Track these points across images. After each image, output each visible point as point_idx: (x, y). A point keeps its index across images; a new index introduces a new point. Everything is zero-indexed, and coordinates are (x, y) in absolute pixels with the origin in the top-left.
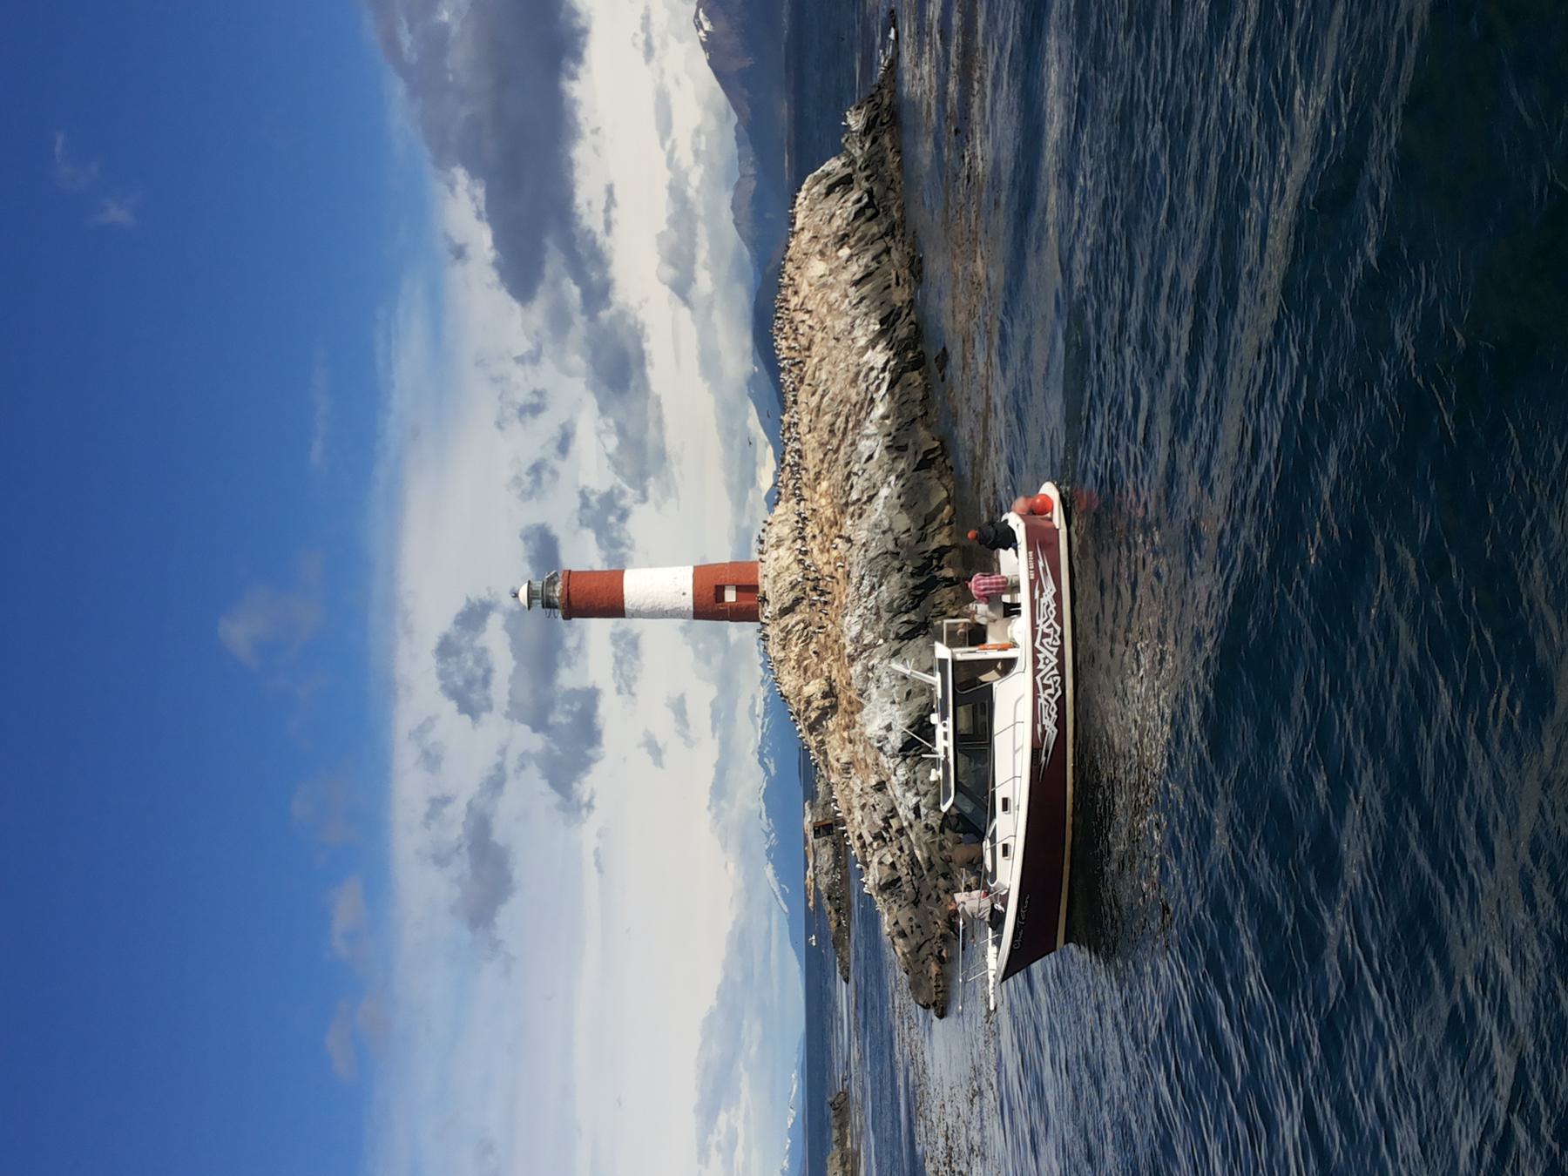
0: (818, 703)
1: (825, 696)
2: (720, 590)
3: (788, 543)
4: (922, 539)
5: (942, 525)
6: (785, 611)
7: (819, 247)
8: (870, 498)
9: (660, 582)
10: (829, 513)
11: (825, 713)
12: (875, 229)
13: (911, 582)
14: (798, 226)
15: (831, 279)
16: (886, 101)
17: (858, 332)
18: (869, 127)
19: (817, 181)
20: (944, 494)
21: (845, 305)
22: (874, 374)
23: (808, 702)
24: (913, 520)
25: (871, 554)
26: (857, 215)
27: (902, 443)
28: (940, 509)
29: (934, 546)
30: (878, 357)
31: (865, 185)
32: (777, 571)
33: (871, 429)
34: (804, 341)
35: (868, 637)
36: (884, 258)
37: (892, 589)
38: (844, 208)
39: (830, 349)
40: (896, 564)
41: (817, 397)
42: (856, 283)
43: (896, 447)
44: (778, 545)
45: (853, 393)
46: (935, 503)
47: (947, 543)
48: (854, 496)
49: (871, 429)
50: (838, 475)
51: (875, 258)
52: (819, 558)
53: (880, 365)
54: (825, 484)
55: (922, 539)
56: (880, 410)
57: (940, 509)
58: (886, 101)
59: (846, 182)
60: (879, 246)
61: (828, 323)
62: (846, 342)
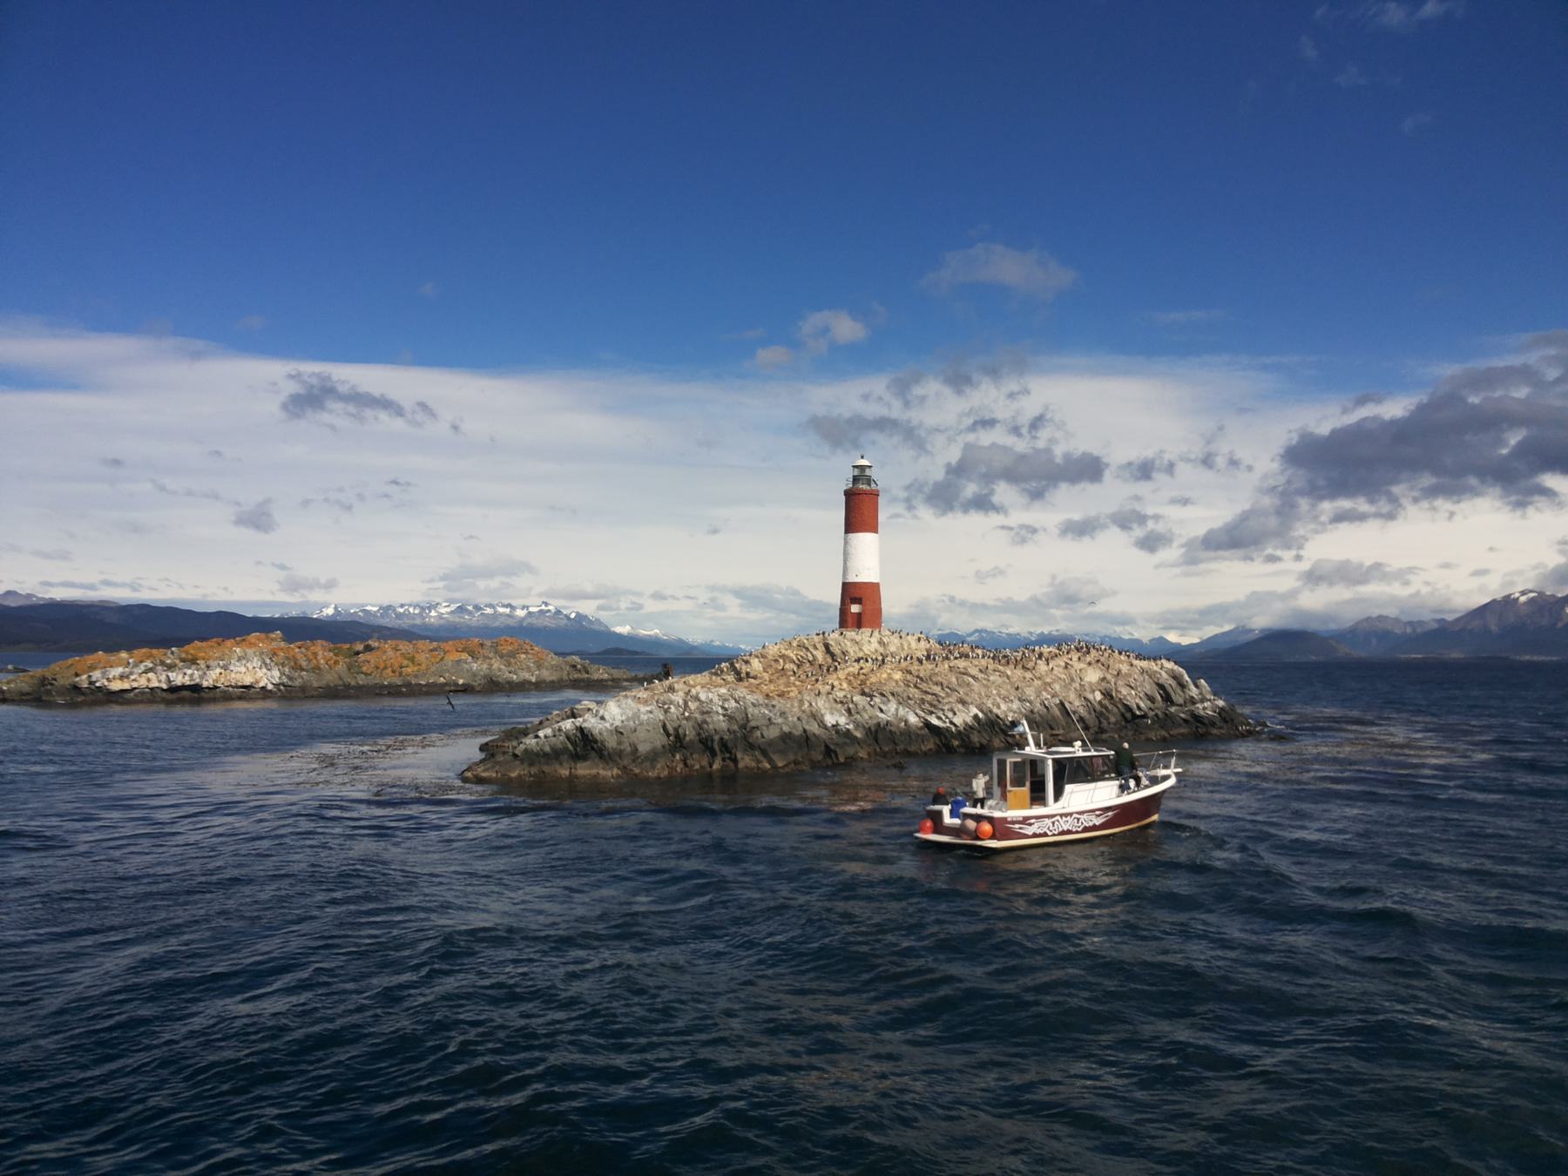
0: (745, 668)
1: (748, 674)
5: (759, 761)
7: (1109, 677)
8: (849, 711)
10: (873, 679)
11: (738, 673)
12: (1113, 719)
13: (716, 738)
16: (1215, 731)
17: (1016, 705)
18: (1197, 718)
19: (1175, 677)
20: (780, 764)
22: (950, 715)
23: (747, 662)
24: (771, 743)
25: (750, 710)
26: (1126, 706)
27: (880, 736)
28: (770, 761)
29: (739, 756)
30: (963, 718)
31: (1151, 714)
32: (867, 642)
33: (902, 712)
34: (1030, 665)
35: (693, 705)
37: (719, 722)
39: (1012, 684)
40: (735, 727)
41: (974, 671)
42: (1062, 704)
43: (878, 734)
44: (881, 642)
45: (953, 699)
46: (775, 757)
47: (741, 765)
48: (857, 698)
49: (902, 712)
50: (886, 689)
51: (1081, 719)
52: (841, 674)
53: (955, 720)
54: (898, 676)
56: (913, 719)
58: (1215, 731)
59: (1167, 698)
60: (1091, 720)
61: (1037, 682)
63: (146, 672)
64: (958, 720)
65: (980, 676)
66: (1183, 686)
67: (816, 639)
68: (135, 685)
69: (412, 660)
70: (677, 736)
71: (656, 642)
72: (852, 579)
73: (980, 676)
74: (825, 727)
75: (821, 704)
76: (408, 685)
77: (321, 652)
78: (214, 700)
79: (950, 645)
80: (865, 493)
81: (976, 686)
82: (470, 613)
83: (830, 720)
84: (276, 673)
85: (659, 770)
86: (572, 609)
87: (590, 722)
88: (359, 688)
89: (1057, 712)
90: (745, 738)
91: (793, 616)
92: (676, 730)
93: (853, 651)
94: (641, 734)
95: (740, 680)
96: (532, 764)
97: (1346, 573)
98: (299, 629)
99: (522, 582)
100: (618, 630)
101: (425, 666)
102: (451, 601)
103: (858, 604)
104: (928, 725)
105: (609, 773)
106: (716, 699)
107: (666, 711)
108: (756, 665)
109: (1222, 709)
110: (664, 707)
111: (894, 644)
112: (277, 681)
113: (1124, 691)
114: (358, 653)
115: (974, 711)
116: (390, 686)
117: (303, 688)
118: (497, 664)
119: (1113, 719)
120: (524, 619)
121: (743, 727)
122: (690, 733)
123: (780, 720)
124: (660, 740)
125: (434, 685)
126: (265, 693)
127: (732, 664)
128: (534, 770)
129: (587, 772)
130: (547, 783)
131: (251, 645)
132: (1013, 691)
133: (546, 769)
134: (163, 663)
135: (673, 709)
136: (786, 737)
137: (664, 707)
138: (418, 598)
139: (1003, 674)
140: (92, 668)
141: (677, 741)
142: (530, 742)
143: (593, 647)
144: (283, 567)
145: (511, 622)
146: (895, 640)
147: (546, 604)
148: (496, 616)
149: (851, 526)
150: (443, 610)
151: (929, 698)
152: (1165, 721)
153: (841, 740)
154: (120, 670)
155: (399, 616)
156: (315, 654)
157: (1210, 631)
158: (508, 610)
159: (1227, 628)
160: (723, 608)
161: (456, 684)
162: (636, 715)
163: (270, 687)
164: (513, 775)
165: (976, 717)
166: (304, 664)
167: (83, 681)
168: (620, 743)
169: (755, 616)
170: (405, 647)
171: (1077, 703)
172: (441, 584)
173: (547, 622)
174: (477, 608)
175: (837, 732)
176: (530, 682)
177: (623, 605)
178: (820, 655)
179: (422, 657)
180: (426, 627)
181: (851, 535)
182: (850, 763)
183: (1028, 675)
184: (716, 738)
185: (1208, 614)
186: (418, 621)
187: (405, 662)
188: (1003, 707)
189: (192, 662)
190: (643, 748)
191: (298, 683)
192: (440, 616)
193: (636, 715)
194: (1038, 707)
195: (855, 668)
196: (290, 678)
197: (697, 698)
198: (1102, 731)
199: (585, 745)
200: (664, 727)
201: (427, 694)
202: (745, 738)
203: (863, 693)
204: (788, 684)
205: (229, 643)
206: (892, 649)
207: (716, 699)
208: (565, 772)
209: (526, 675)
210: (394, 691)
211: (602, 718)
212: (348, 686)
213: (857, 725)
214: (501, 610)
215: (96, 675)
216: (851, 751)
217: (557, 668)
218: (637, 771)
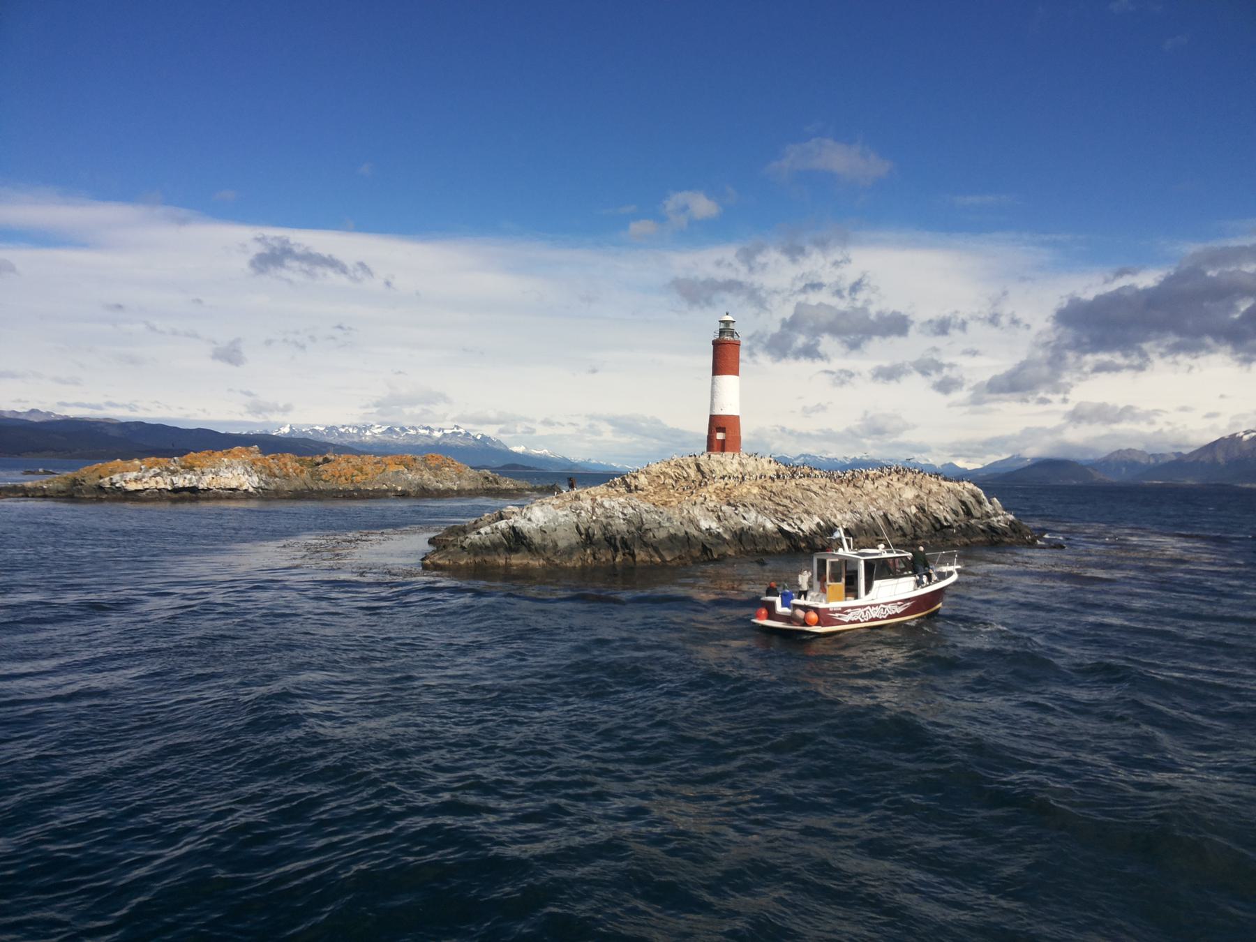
0: (633, 482)
2: (722, 430)
3: (741, 469)
4: (646, 544)
5: (651, 556)
6: (698, 466)
7: (922, 495)
8: (719, 517)
9: (731, 395)
10: (736, 493)
11: (628, 486)
12: (925, 529)
13: (618, 537)
14: (943, 483)
15: (896, 501)
16: (1007, 540)
17: (849, 516)
18: (992, 529)
21: (872, 508)
22: (798, 522)
23: (635, 477)
24: (661, 542)
25: (645, 515)
27: (744, 538)
28: (661, 556)
30: (808, 525)
31: (955, 525)
33: (760, 519)
34: (859, 484)
35: (599, 511)
36: (900, 533)
37: (619, 525)
38: (943, 511)
40: (633, 529)
42: (885, 515)
43: (742, 536)
44: (741, 464)
47: (638, 559)
48: (725, 508)
49: (760, 519)
50: (747, 501)
51: (901, 528)
52: (711, 488)
53: (803, 527)
54: (755, 490)
55: (646, 544)
56: (769, 526)
57: (661, 556)
58: (1007, 540)
59: (968, 513)
60: (908, 528)
61: (865, 498)
62: (846, 507)
63: (155, 476)
64: (805, 527)
65: (820, 492)
66: (980, 503)
67: (690, 460)
68: (147, 486)
69: (361, 470)
70: (587, 535)
71: (545, 460)
72: (717, 412)
73: (820, 492)
74: (701, 530)
75: (697, 512)
76: (359, 490)
77: (290, 463)
78: (208, 499)
79: (791, 468)
80: (729, 343)
81: (817, 499)
82: (397, 433)
83: (704, 525)
84: (255, 479)
85: (575, 562)
86: (479, 431)
87: (521, 523)
88: (320, 492)
89: (880, 522)
90: (641, 537)
91: (655, 441)
92: (587, 530)
93: (719, 471)
94: (560, 533)
95: (630, 491)
96: (476, 555)
97: (1101, 414)
98: (269, 445)
99: (439, 409)
100: (516, 449)
101: (371, 475)
102: (383, 424)
103: (722, 433)
104: (781, 530)
105: (536, 563)
106: (617, 507)
107: (578, 515)
108: (643, 480)
109: (1012, 522)
110: (577, 511)
111: (751, 465)
112: (256, 485)
113: (935, 506)
114: (318, 464)
115: (817, 519)
116: (344, 491)
117: (277, 491)
118: (427, 475)
119: (925, 529)
120: (440, 439)
121: (639, 529)
122: (598, 534)
123: (667, 524)
124: (575, 539)
125: (379, 491)
126: (247, 495)
127: (623, 479)
128: (478, 559)
129: (518, 562)
130: (493, 571)
131: (235, 456)
132: (846, 504)
133: (488, 558)
134: (167, 469)
135: (583, 514)
136: (672, 538)
137: (577, 511)
138: (356, 421)
139: (838, 490)
140: (113, 472)
141: (587, 539)
142: (473, 537)
143: (496, 463)
144: (249, 394)
145: (430, 442)
146: (752, 462)
147: (458, 428)
148: (418, 436)
149: (718, 370)
150: (376, 431)
151: (781, 508)
152: (967, 530)
153: (715, 541)
154: (135, 474)
155: (341, 435)
156: (285, 464)
157: (991, 459)
158: (427, 432)
159: (1005, 456)
160: (599, 433)
161: (396, 491)
162: (555, 519)
163: (251, 490)
164: (462, 563)
165: (818, 524)
166: (277, 472)
167: (106, 482)
168: (544, 540)
169: (624, 439)
170: (355, 460)
171: (897, 515)
172: (375, 410)
173: (459, 442)
174: (403, 429)
175: (710, 534)
176: (452, 490)
177: (519, 429)
178: (692, 472)
179: (368, 469)
180: (362, 444)
181: (717, 377)
182: (722, 558)
183: (858, 492)
184: (618, 537)
185: (990, 445)
186: (356, 440)
187: (356, 472)
188: (839, 517)
189: (191, 468)
190: (562, 544)
191: (273, 487)
192: (374, 435)
193: (555, 519)
194: (866, 518)
195: (721, 484)
196: (266, 483)
197: (602, 505)
198: (916, 537)
199: (517, 540)
200: (577, 527)
201: (373, 497)
202: (641, 537)
203: (729, 504)
204: (669, 496)
205: (218, 454)
206: (750, 469)
207: (617, 507)
208: (502, 562)
209: (449, 485)
210: (348, 495)
211: (529, 520)
212: (311, 490)
213: (726, 529)
214: (422, 431)
215: (116, 477)
216: (723, 549)
217: (473, 479)
218: (558, 562)
